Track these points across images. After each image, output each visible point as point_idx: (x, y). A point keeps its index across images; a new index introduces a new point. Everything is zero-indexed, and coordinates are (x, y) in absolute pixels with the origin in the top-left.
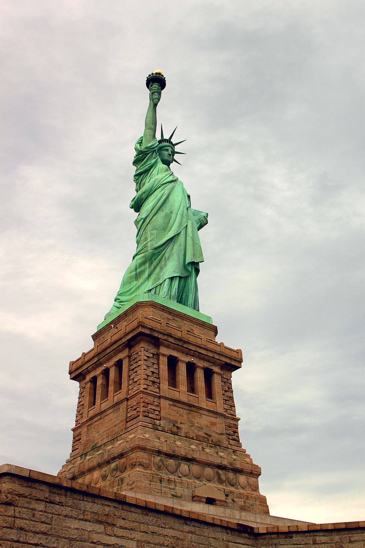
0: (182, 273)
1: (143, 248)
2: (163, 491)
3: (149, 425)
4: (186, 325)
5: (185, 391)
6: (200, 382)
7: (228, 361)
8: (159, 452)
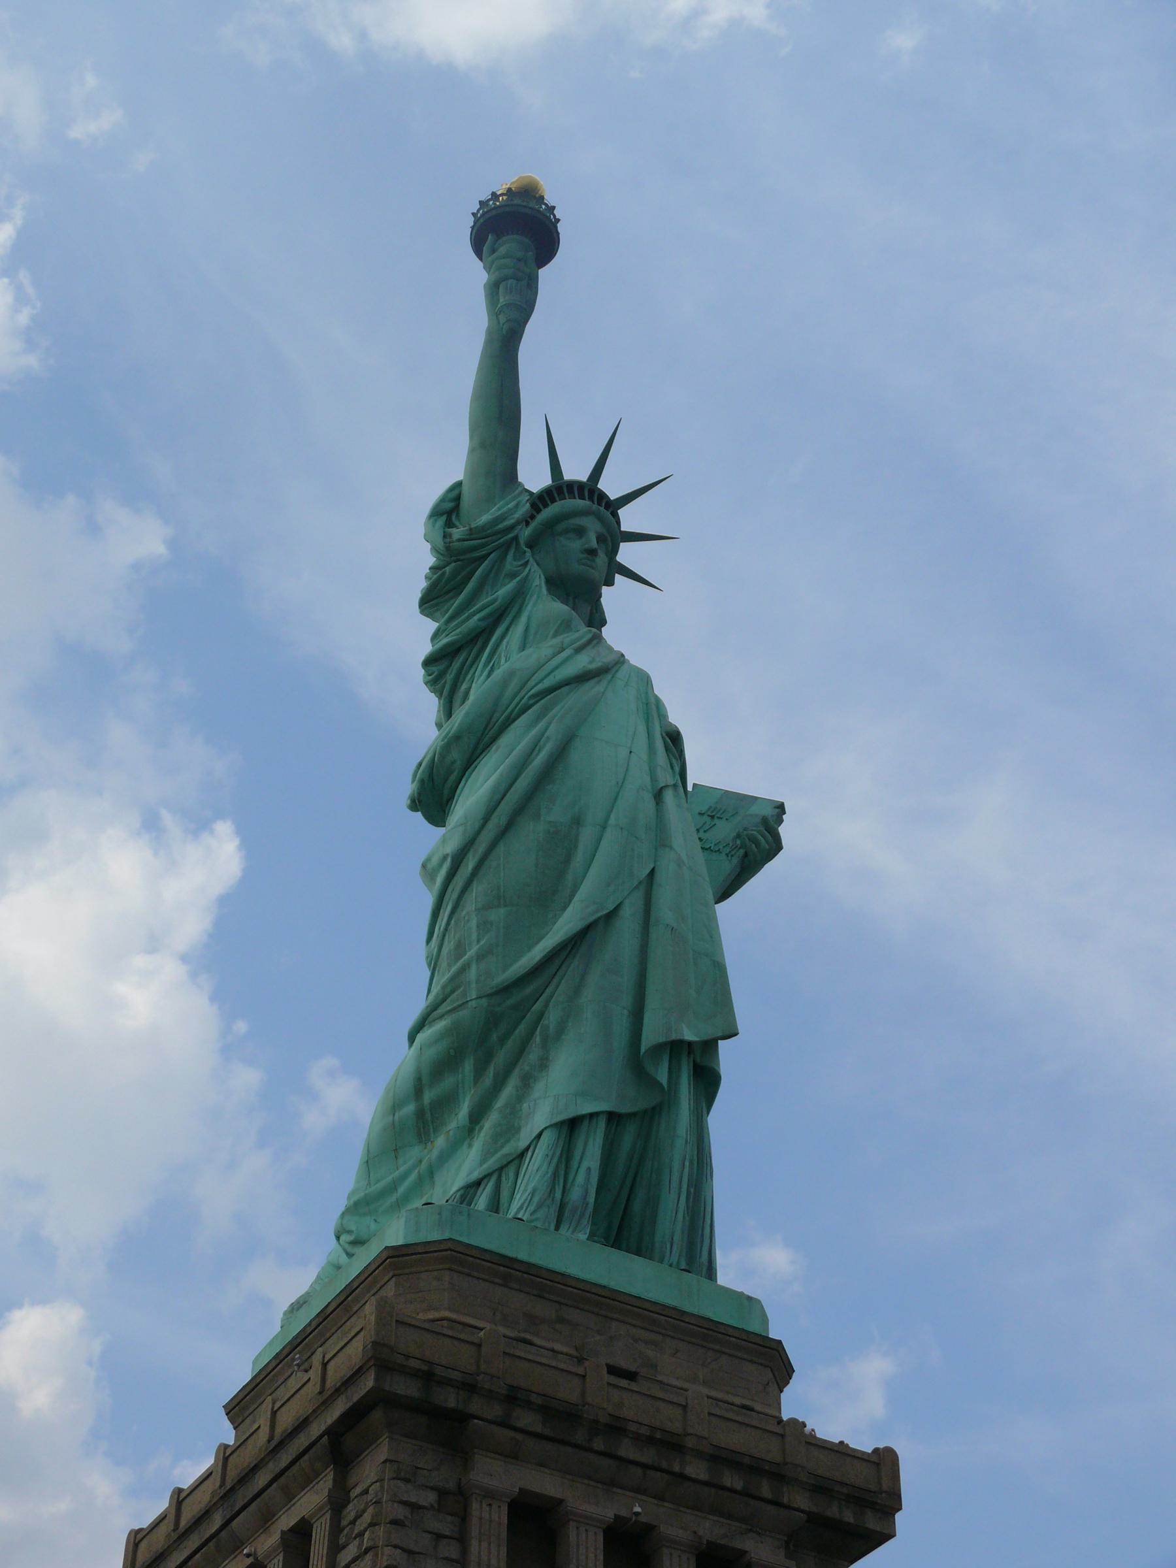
1: (448, 989)
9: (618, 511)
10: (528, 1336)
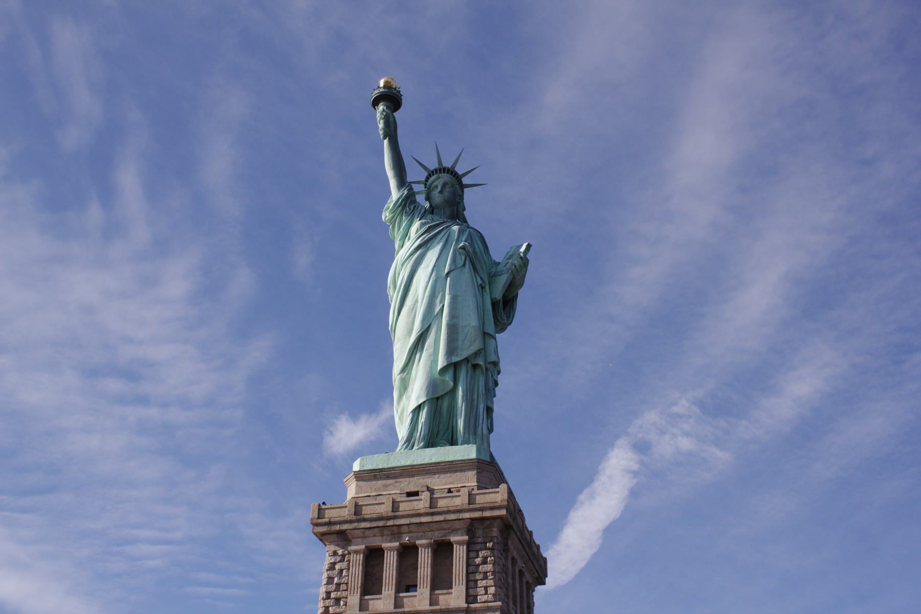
4: (413, 483)
6: (422, 569)
7: (477, 515)
9: (455, 169)
10: (381, 493)
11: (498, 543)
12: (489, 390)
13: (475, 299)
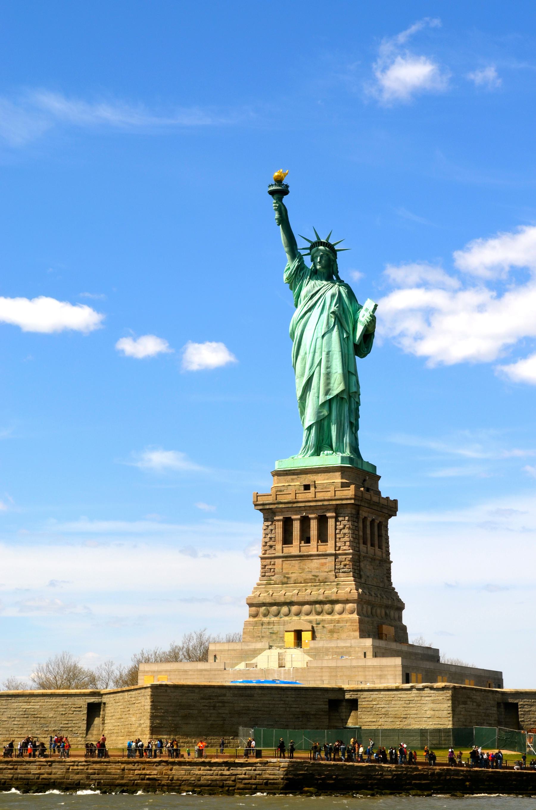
0: (318, 417)
2: (263, 632)
3: (263, 583)
4: (307, 480)
5: (297, 545)
6: (313, 531)
8: (264, 604)
11: (352, 517)
12: (352, 411)
13: (340, 353)
